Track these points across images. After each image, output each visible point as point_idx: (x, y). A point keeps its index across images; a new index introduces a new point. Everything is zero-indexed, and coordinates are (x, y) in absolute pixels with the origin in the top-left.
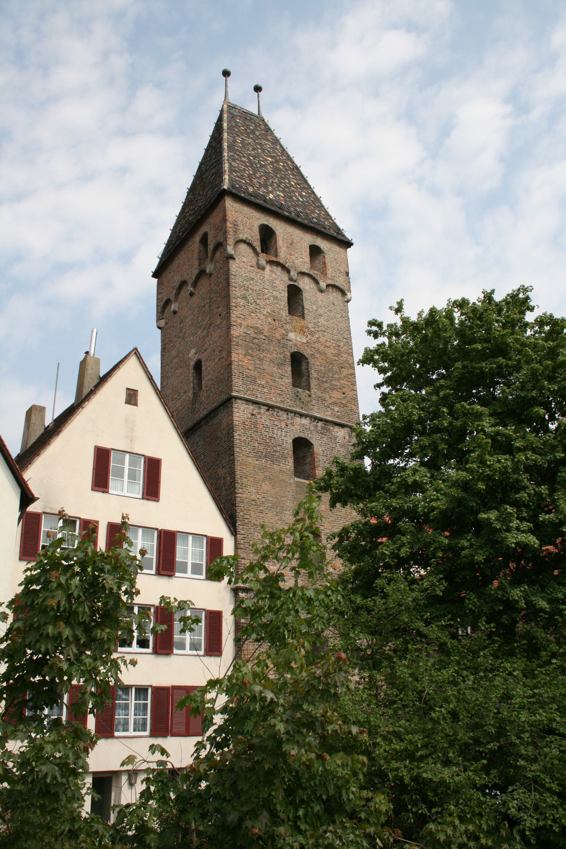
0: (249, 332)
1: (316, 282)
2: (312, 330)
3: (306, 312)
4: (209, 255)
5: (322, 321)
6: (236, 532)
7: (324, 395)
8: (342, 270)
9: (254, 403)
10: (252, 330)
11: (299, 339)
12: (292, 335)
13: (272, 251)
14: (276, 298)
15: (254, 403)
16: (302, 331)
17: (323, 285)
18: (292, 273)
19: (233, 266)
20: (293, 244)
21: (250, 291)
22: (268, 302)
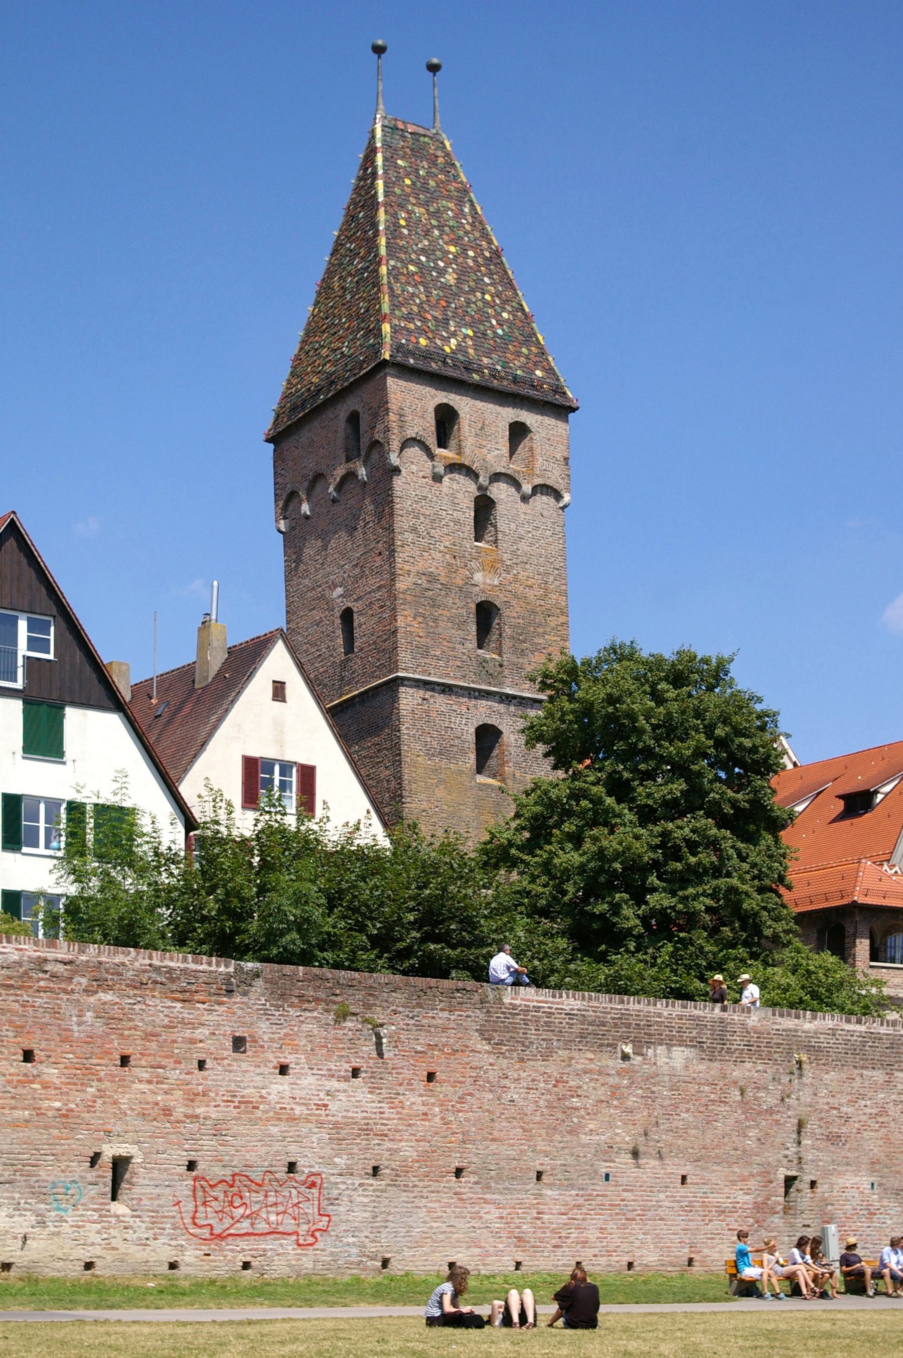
0: (420, 582)
1: (517, 485)
2: (508, 563)
3: (500, 536)
4: (363, 453)
5: (523, 546)
7: (521, 660)
10: (423, 577)
11: (488, 581)
12: (478, 577)
13: (453, 443)
16: (492, 567)
17: (527, 488)
18: (481, 479)
19: (398, 483)
20: (483, 425)
21: (422, 518)
22: (446, 532)
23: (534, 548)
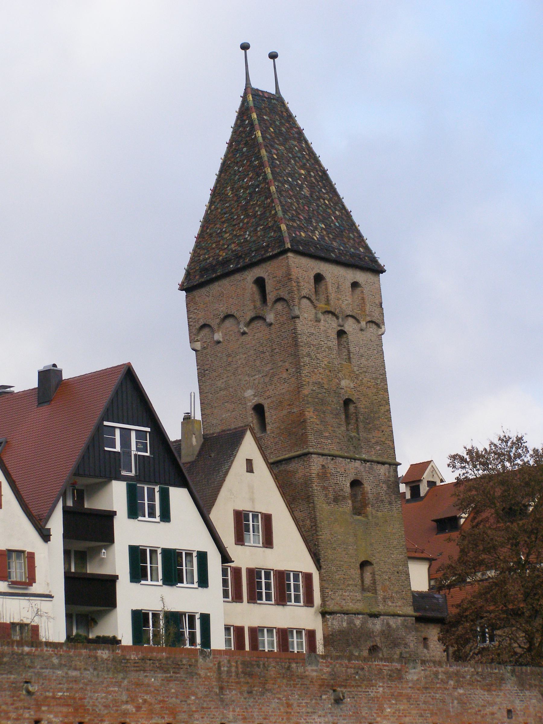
0: (314, 388)
3: (352, 355)
6: (320, 567)
7: (369, 436)
8: (377, 302)
9: (323, 455)
14: (329, 348)
15: (323, 455)
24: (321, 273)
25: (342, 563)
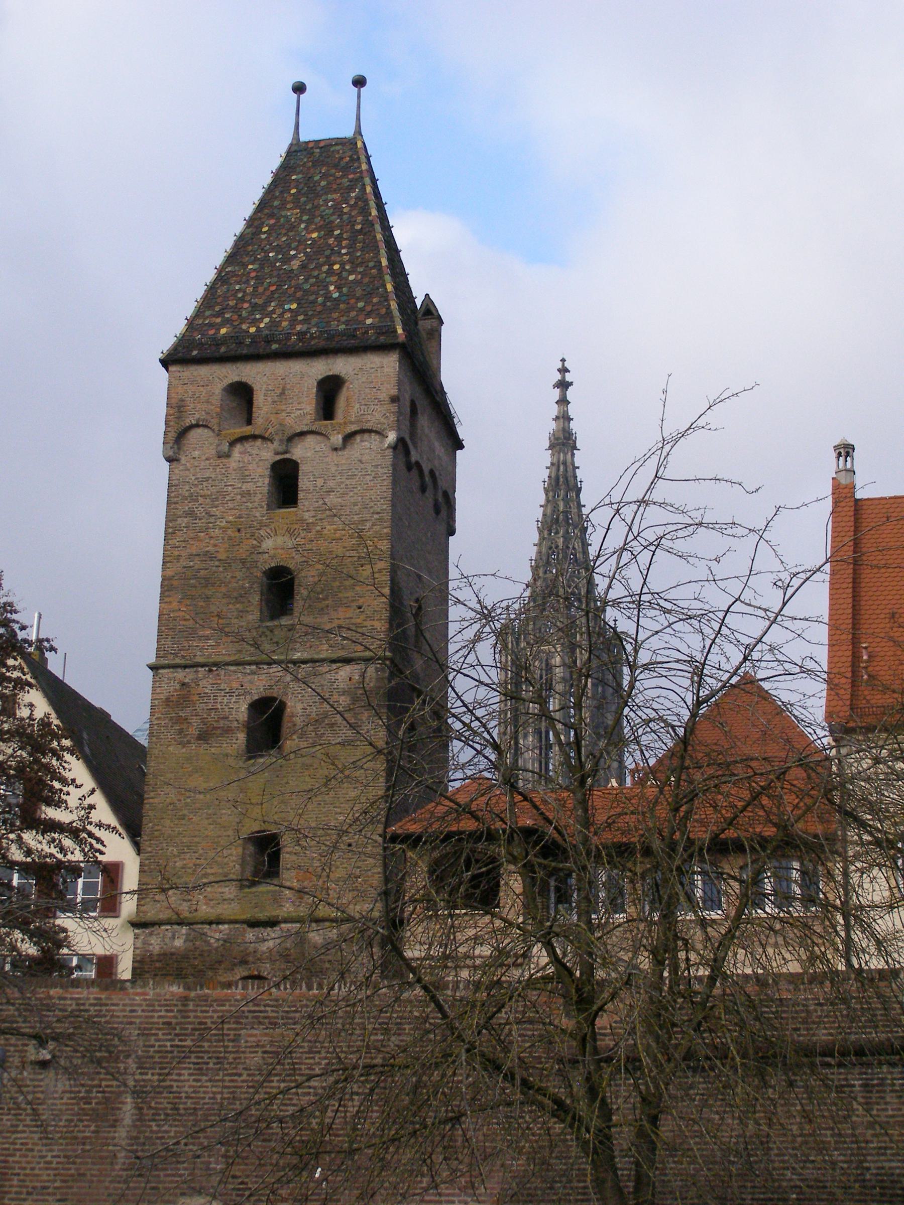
7: (319, 620)
10: (197, 558)
12: (268, 544)
23: (347, 498)
24: (244, 380)
25: (196, 840)
